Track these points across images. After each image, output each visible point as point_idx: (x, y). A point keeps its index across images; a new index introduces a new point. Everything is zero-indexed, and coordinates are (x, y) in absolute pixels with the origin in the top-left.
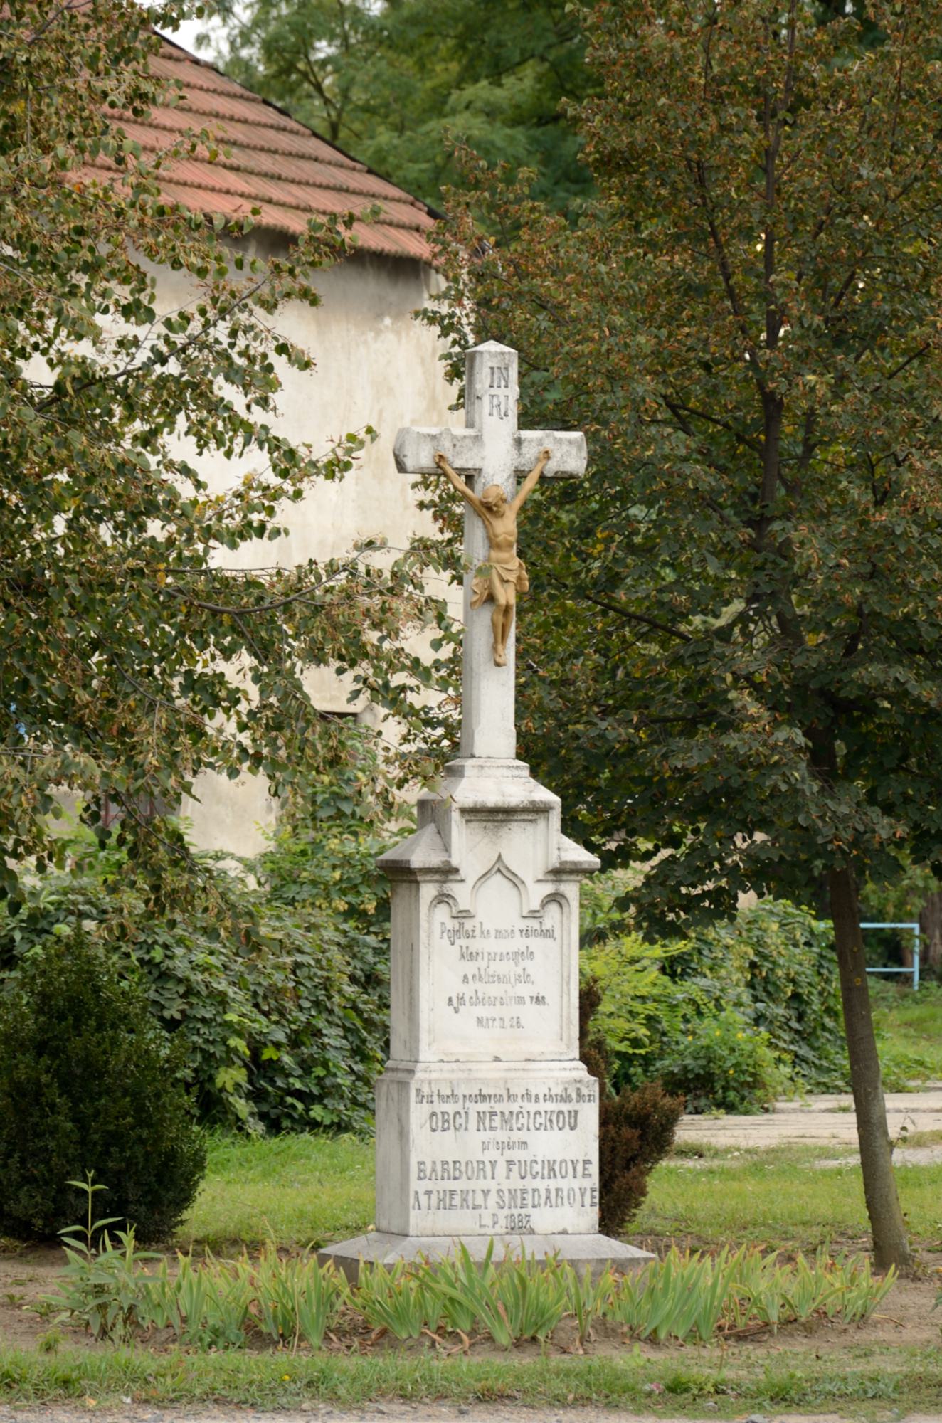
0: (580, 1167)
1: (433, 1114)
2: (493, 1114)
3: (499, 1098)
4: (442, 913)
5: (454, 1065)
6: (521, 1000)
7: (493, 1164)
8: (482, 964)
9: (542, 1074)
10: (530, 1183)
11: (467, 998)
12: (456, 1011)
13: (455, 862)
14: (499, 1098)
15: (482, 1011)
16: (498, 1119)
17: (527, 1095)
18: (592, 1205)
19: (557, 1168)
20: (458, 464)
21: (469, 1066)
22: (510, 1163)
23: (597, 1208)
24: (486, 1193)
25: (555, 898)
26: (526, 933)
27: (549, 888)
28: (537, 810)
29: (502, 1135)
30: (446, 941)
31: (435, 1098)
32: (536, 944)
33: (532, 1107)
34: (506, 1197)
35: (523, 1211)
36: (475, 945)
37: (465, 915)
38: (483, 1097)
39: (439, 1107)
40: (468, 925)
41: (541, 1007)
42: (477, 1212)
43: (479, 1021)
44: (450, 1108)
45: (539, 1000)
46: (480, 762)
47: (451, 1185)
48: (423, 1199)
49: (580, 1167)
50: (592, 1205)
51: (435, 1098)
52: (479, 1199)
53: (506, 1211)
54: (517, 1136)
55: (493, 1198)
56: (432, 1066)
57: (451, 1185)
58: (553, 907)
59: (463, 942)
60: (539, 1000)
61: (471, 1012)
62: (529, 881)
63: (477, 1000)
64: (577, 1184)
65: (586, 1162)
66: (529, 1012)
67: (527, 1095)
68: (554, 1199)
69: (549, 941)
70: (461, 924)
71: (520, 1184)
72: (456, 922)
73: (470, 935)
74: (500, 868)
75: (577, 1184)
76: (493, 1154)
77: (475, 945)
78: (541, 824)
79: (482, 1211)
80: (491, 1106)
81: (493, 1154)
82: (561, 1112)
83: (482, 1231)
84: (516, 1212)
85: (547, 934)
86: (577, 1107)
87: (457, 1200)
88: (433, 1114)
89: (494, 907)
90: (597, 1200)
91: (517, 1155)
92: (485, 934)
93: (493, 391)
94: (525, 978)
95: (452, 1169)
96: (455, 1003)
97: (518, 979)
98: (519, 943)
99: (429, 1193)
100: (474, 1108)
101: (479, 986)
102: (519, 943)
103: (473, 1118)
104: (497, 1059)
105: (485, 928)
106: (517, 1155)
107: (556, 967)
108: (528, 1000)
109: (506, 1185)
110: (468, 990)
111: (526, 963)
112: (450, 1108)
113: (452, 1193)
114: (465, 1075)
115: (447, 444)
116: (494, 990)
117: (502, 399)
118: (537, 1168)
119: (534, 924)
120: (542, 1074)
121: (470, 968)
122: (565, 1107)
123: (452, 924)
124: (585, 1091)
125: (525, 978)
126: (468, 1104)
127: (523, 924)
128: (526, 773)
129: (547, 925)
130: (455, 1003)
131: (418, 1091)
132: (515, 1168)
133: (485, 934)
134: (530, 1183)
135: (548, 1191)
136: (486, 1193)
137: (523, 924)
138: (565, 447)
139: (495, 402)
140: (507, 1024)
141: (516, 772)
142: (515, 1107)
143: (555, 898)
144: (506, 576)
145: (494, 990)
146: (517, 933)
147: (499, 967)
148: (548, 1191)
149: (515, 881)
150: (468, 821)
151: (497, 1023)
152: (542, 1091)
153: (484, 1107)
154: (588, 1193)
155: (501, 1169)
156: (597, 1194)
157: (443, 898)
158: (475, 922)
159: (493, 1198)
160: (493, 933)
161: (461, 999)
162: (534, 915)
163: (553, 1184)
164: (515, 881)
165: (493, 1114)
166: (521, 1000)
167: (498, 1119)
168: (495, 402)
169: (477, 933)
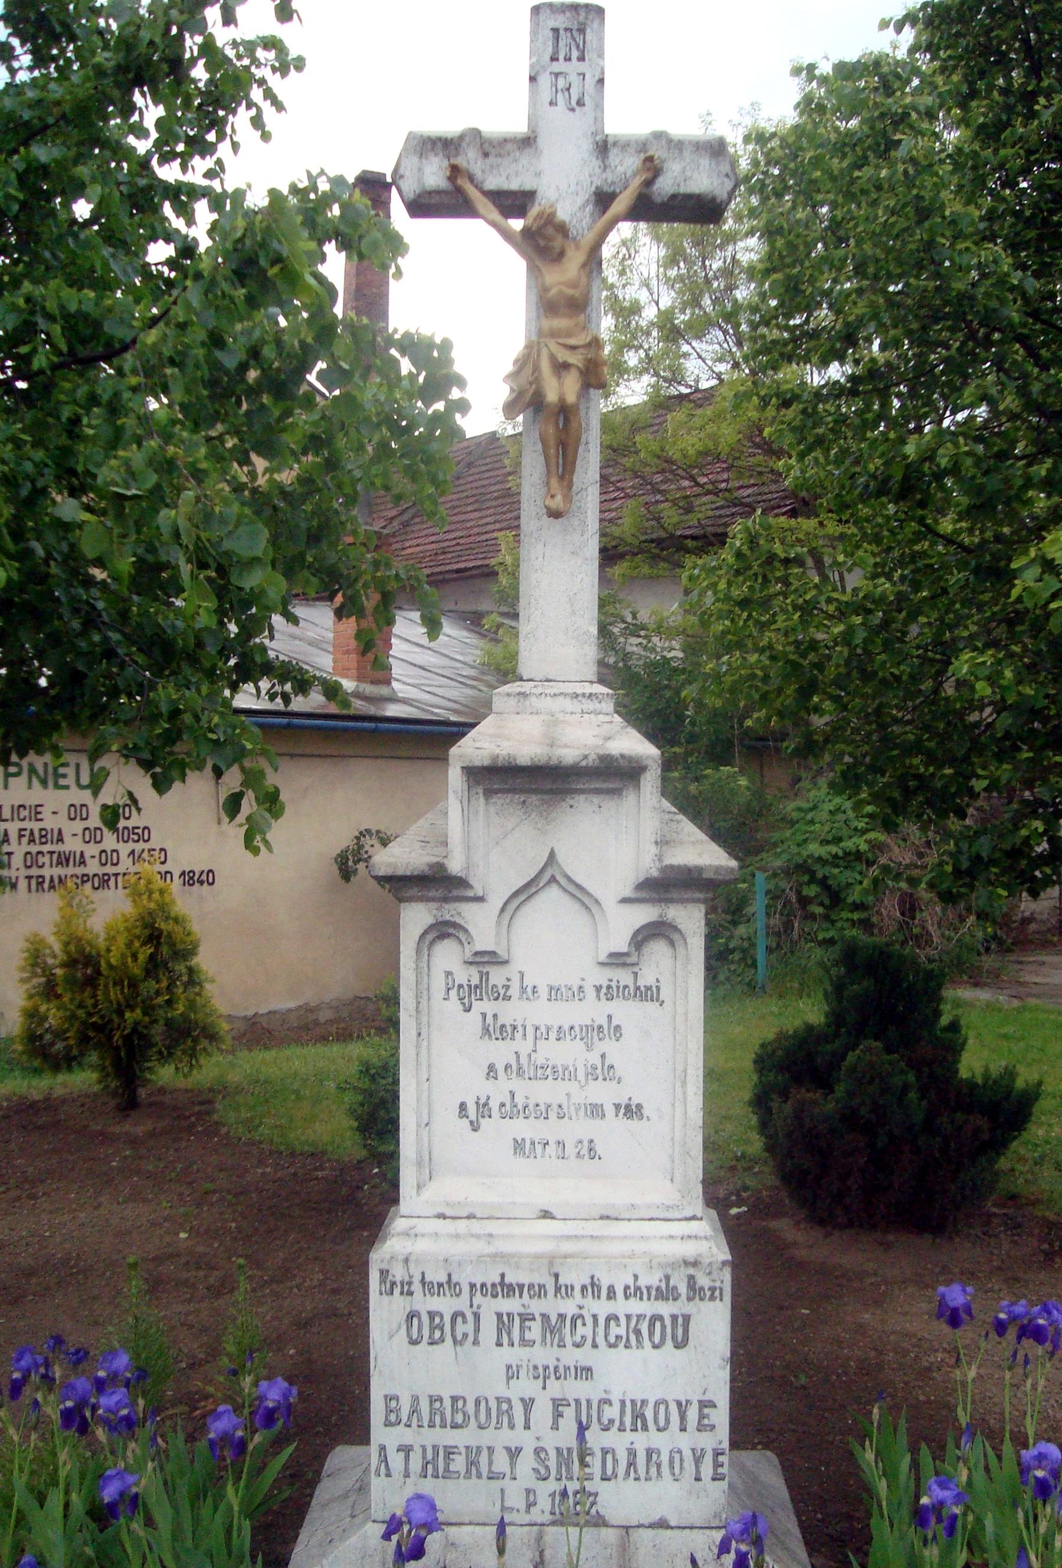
0: (693, 1414)
3: (540, 1291)
4: (447, 957)
5: (462, 1226)
6: (596, 1111)
7: (528, 1404)
8: (524, 1046)
11: (494, 1105)
12: (475, 1127)
13: (455, 866)
14: (540, 1291)
15: (523, 1128)
16: (535, 1330)
19: (649, 1413)
20: (492, 183)
21: (492, 1227)
22: (558, 1404)
23: (724, 1485)
24: (514, 1454)
25: (657, 931)
26: (608, 992)
27: (644, 914)
28: (613, 775)
29: (543, 1355)
30: (454, 1004)
31: (417, 1287)
32: (625, 1011)
33: (602, 1308)
34: (552, 1463)
36: (511, 1012)
38: (506, 1288)
39: (424, 1303)
40: (497, 976)
41: (634, 1124)
42: (496, 1484)
43: (518, 1146)
44: (445, 1305)
45: (631, 1111)
46: (527, 687)
48: (396, 1461)
49: (693, 1414)
51: (417, 1287)
52: (502, 1462)
53: (552, 1485)
54: (571, 1356)
55: (526, 1463)
59: (487, 1006)
60: (631, 1111)
63: (512, 1110)
64: (685, 1442)
65: (704, 1404)
66: (613, 1132)
67: (592, 1288)
68: (643, 1466)
69: (651, 1007)
70: (484, 976)
73: (501, 995)
75: (685, 1442)
76: (526, 1386)
77: (511, 1012)
80: (525, 1304)
81: (526, 1386)
82: (656, 1318)
85: (648, 994)
86: (688, 1308)
87: (459, 1463)
88: (411, 1316)
89: (554, 949)
91: (574, 1389)
92: (529, 993)
93: (556, 67)
94: (605, 1071)
95: (446, 1411)
96: (475, 1114)
97: (592, 1074)
98: (592, 1010)
99: (406, 1450)
100: (490, 1307)
102: (592, 1010)
103: (489, 1325)
104: (546, 1215)
105: (528, 982)
106: (574, 1389)
108: (610, 1110)
109: (551, 1441)
110: (497, 1092)
111: (608, 1046)
112: (445, 1305)
114: (481, 1247)
116: (544, 1092)
117: (574, 79)
118: (612, 1412)
119: (624, 977)
121: (501, 1052)
122: (665, 1309)
123: (464, 975)
124: (703, 1281)
125: (605, 1071)
126: (478, 1299)
127: (602, 977)
128: (609, 706)
129: (647, 978)
130: (475, 1114)
131: (384, 1273)
132: (569, 1413)
133: (529, 993)
135: (632, 1453)
136: (514, 1454)
137: (602, 977)
139: (561, 83)
140: (571, 1150)
141: (590, 705)
142: (569, 1307)
143: (657, 931)
145: (544, 1092)
146: (591, 993)
147: (552, 1052)
148: (632, 1453)
149: (581, 895)
152: (621, 1280)
154: (708, 1459)
155: (542, 1412)
157: (443, 931)
158: (511, 972)
159: (526, 1463)
160: (543, 992)
161: (483, 1107)
162: (617, 960)
163: (641, 1441)
164: (581, 895)
165: (526, 1318)
166: (596, 1111)
168: (561, 83)
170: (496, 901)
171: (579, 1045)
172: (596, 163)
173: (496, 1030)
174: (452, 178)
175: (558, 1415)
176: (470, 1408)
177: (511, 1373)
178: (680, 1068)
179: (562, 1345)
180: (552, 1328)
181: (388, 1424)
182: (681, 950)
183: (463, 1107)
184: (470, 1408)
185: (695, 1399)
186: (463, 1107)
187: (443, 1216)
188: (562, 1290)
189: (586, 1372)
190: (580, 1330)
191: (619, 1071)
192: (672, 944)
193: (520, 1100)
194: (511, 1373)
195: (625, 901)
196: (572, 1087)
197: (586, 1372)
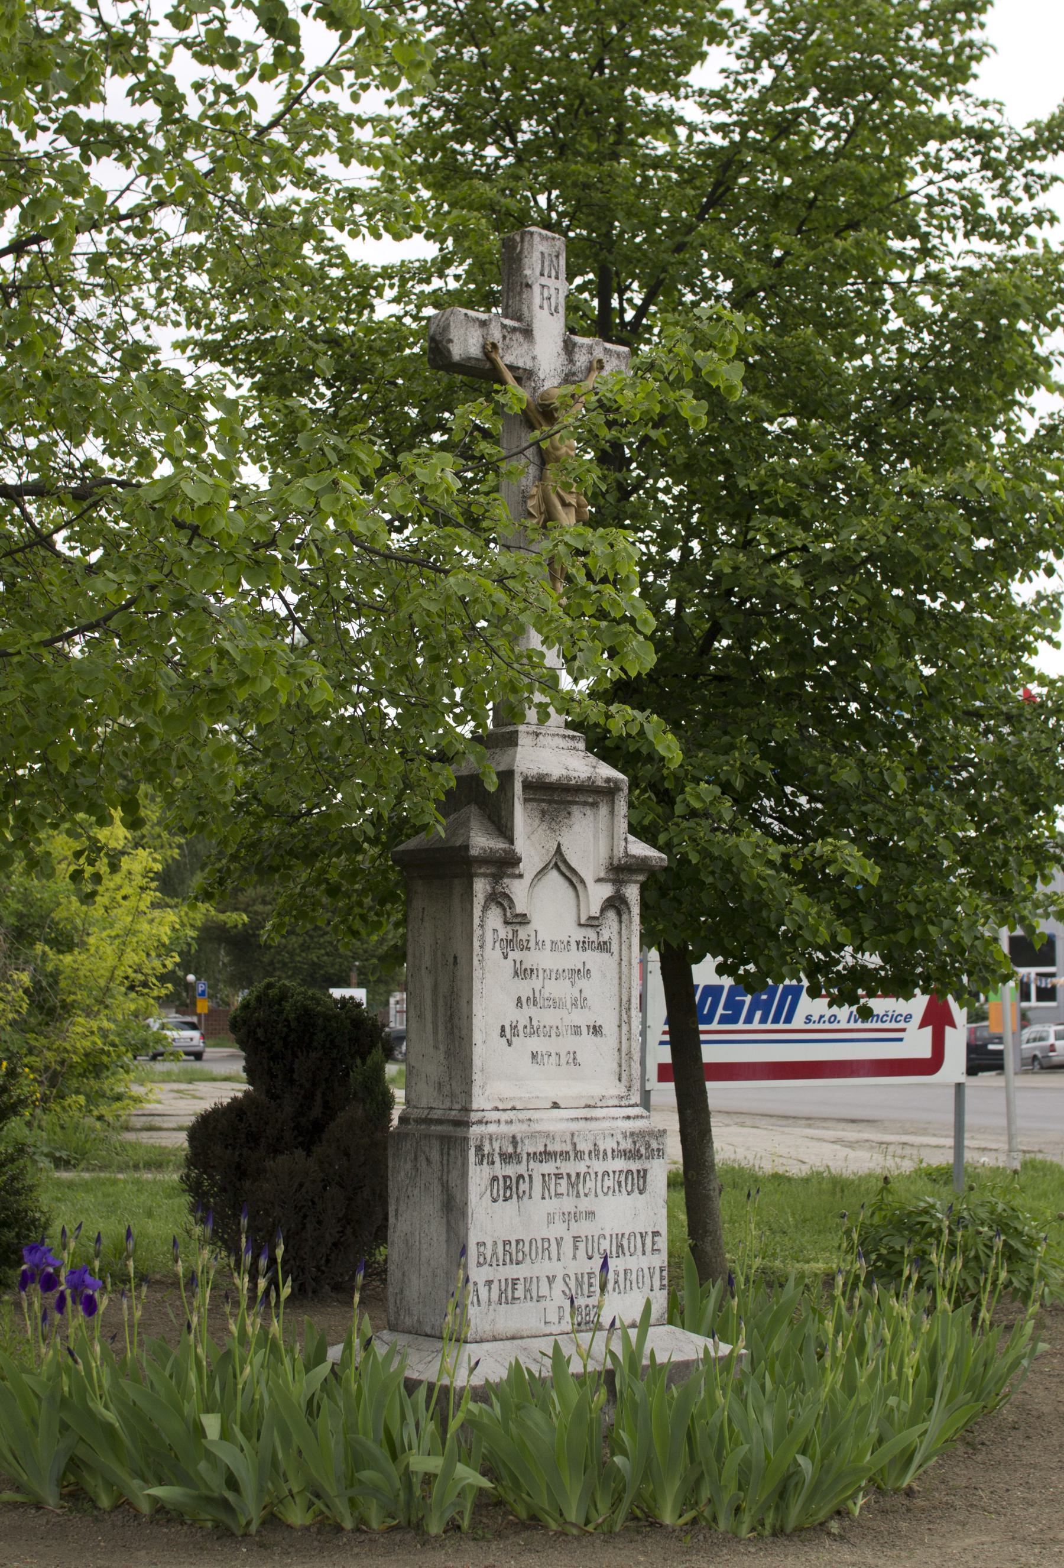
0: (648, 1241)
1: (495, 1179)
2: (558, 1176)
3: (565, 1155)
5: (511, 1115)
6: (577, 1030)
7: (559, 1242)
8: (536, 983)
9: (606, 1124)
11: (520, 1027)
14: (565, 1155)
15: (535, 1044)
17: (596, 1153)
19: (625, 1243)
22: (576, 1239)
26: (583, 945)
27: (607, 891)
29: (568, 1204)
30: (498, 953)
31: (497, 1159)
32: (594, 959)
33: (599, 1166)
36: (532, 959)
38: (547, 1155)
39: (500, 1169)
40: (522, 934)
41: (598, 1040)
42: (543, 1304)
43: (534, 1056)
44: (511, 1170)
45: (596, 1030)
47: (511, 1271)
48: (483, 1292)
49: (648, 1241)
54: (585, 1204)
57: (511, 1271)
60: (596, 1030)
62: (589, 880)
63: (532, 1030)
64: (645, 1262)
65: (656, 1234)
67: (596, 1153)
69: (605, 956)
72: (509, 928)
73: (524, 947)
74: (559, 863)
75: (645, 1262)
76: (559, 1229)
77: (532, 959)
78: (604, 810)
81: (559, 1229)
82: (630, 1172)
85: (604, 947)
86: (647, 1165)
88: (495, 1179)
91: (584, 1228)
92: (540, 945)
94: (580, 1002)
95: (513, 1251)
96: (508, 1033)
98: (575, 959)
99: (489, 1283)
101: (533, 1011)
104: (556, 1106)
105: (540, 938)
106: (584, 1228)
108: (584, 1029)
111: (582, 983)
112: (511, 1170)
113: (515, 1281)
116: (547, 1017)
117: (553, 292)
119: (591, 934)
121: (524, 987)
122: (634, 1166)
123: (504, 932)
125: (580, 1002)
126: (532, 1164)
127: (579, 934)
128: (581, 745)
129: (605, 936)
130: (508, 1033)
131: (479, 1148)
132: (582, 1246)
133: (540, 945)
136: (551, 1280)
137: (579, 934)
140: (563, 1061)
141: (571, 744)
142: (581, 1167)
146: (574, 946)
149: (572, 878)
152: (608, 1145)
153: (549, 1168)
155: (567, 1246)
158: (529, 929)
162: (593, 923)
164: (572, 878)
165: (558, 1176)
166: (577, 1030)
167: (564, 1182)
169: (532, 944)
170: (528, 877)
171: (568, 982)
172: (563, 356)
173: (522, 972)
174: (486, 354)
175: (576, 1248)
176: (527, 1249)
177: (550, 1219)
178: (625, 999)
179: (578, 1195)
180: (575, 1181)
181: (479, 1265)
182: (625, 917)
183: (503, 1028)
184: (527, 1249)
185: (650, 1230)
186: (503, 1028)
187: (497, 1109)
188: (579, 1155)
189: (591, 1214)
190: (589, 1184)
191: (589, 1003)
192: (619, 914)
193: (535, 1023)
194: (550, 1219)
195: (599, 880)
196: (563, 1013)
197: (591, 1214)
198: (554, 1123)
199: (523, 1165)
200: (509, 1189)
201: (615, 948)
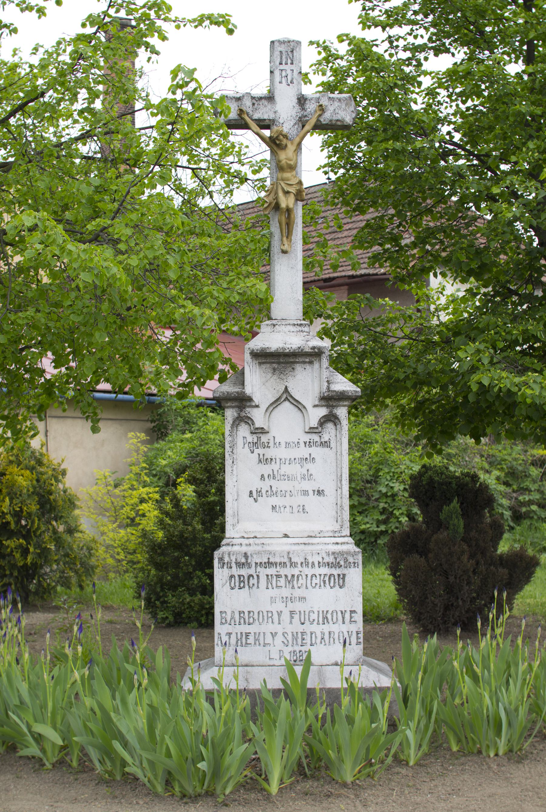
0: (347, 616)
1: (232, 576)
2: (278, 576)
4: (243, 431)
5: (251, 541)
6: (305, 493)
7: (279, 614)
8: (275, 467)
9: (319, 547)
10: (308, 628)
11: (264, 492)
12: (256, 500)
15: (274, 501)
16: (282, 581)
17: (306, 563)
18: (358, 643)
19: (329, 616)
20: (256, 116)
21: (262, 541)
22: (292, 613)
23: (361, 646)
24: (274, 635)
26: (309, 444)
27: (323, 412)
29: (286, 592)
31: (234, 565)
32: (317, 452)
33: (309, 571)
34: (290, 637)
35: (303, 649)
37: (262, 431)
38: (269, 564)
39: (235, 571)
41: (321, 498)
42: (267, 648)
43: (274, 508)
45: (320, 493)
46: (274, 322)
47: (245, 629)
49: (347, 616)
50: (358, 643)
51: (234, 565)
52: (269, 639)
53: (290, 648)
54: (298, 593)
55: (279, 639)
56: (235, 541)
57: (245, 629)
58: (330, 426)
59: (261, 451)
60: (320, 493)
61: (267, 502)
62: (309, 406)
63: (271, 492)
64: (344, 628)
65: (352, 612)
66: (312, 501)
67: (306, 563)
68: (327, 639)
69: (326, 450)
70: (259, 438)
71: (301, 628)
72: (255, 436)
73: (266, 446)
74: (286, 396)
75: (344, 628)
76: (279, 606)
77: (270, 453)
78: (316, 365)
79: (271, 648)
81: (279, 606)
83: (271, 663)
84: (297, 648)
85: (325, 444)
86: (345, 571)
87: (251, 640)
88: (232, 576)
89: (286, 427)
90: (361, 640)
91: (298, 606)
93: (281, 67)
94: (308, 476)
96: (255, 495)
97: (303, 478)
98: (304, 452)
99: (229, 634)
100: (263, 572)
101: (272, 482)
102: (304, 452)
103: (263, 579)
104: (286, 536)
105: (277, 440)
106: (298, 606)
107: (330, 468)
108: (311, 493)
109: (289, 629)
110: (265, 486)
111: (310, 466)
112: (244, 572)
113: (247, 635)
114: (259, 548)
115: (247, 103)
116: (284, 486)
117: (289, 72)
118: (314, 616)
119: (316, 438)
120: (319, 547)
121: (266, 469)
122: (335, 572)
123: (250, 438)
124: (351, 560)
125: (308, 476)
126: (259, 569)
129: (326, 438)
130: (255, 495)
132: (296, 617)
134: (308, 628)
135: (323, 633)
136: (274, 635)
138: (337, 104)
139: (284, 74)
140: (296, 510)
142: (296, 572)
144: (287, 188)
145: (284, 486)
146: (302, 444)
147: (286, 469)
148: (323, 633)
149: (298, 405)
150: (260, 364)
151: (288, 509)
152: (316, 559)
153: (272, 571)
154: (354, 635)
155: (286, 616)
156: (361, 635)
158: (270, 436)
159: (279, 639)
160: (283, 444)
161: (259, 492)
162: (312, 431)
163: (326, 628)
164: (298, 405)
165: (278, 576)
166: (305, 493)
167: (282, 581)
168: (284, 74)
169: (271, 444)
170: (263, 407)
171: (298, 466)
172: (297, 107)
173: (263, 460)
174: (239, 115)
175: (292, 618)
176: (256, 616)
177: (273, 600)
178: (339, 474)
179: (293, 587)
180: (290, 580)
181: (222, 623)
182: (338, 426)
183: (251, 492)
184: (256, 616)
185: (348, 610)
186: (251, 492)
187: (244, 537)
188: (293, 565)
189: (302, 599)
190: (301, 581)
191: (314, 476)
192: (335, 425)
193: (274, 489)
194: (273, 600)
195: (315, 406)
196: (295, 483)
197: (302, 599)
198: (280, 547)
199: (279, 568)
200: (243, 582)
201: (333, 445)
